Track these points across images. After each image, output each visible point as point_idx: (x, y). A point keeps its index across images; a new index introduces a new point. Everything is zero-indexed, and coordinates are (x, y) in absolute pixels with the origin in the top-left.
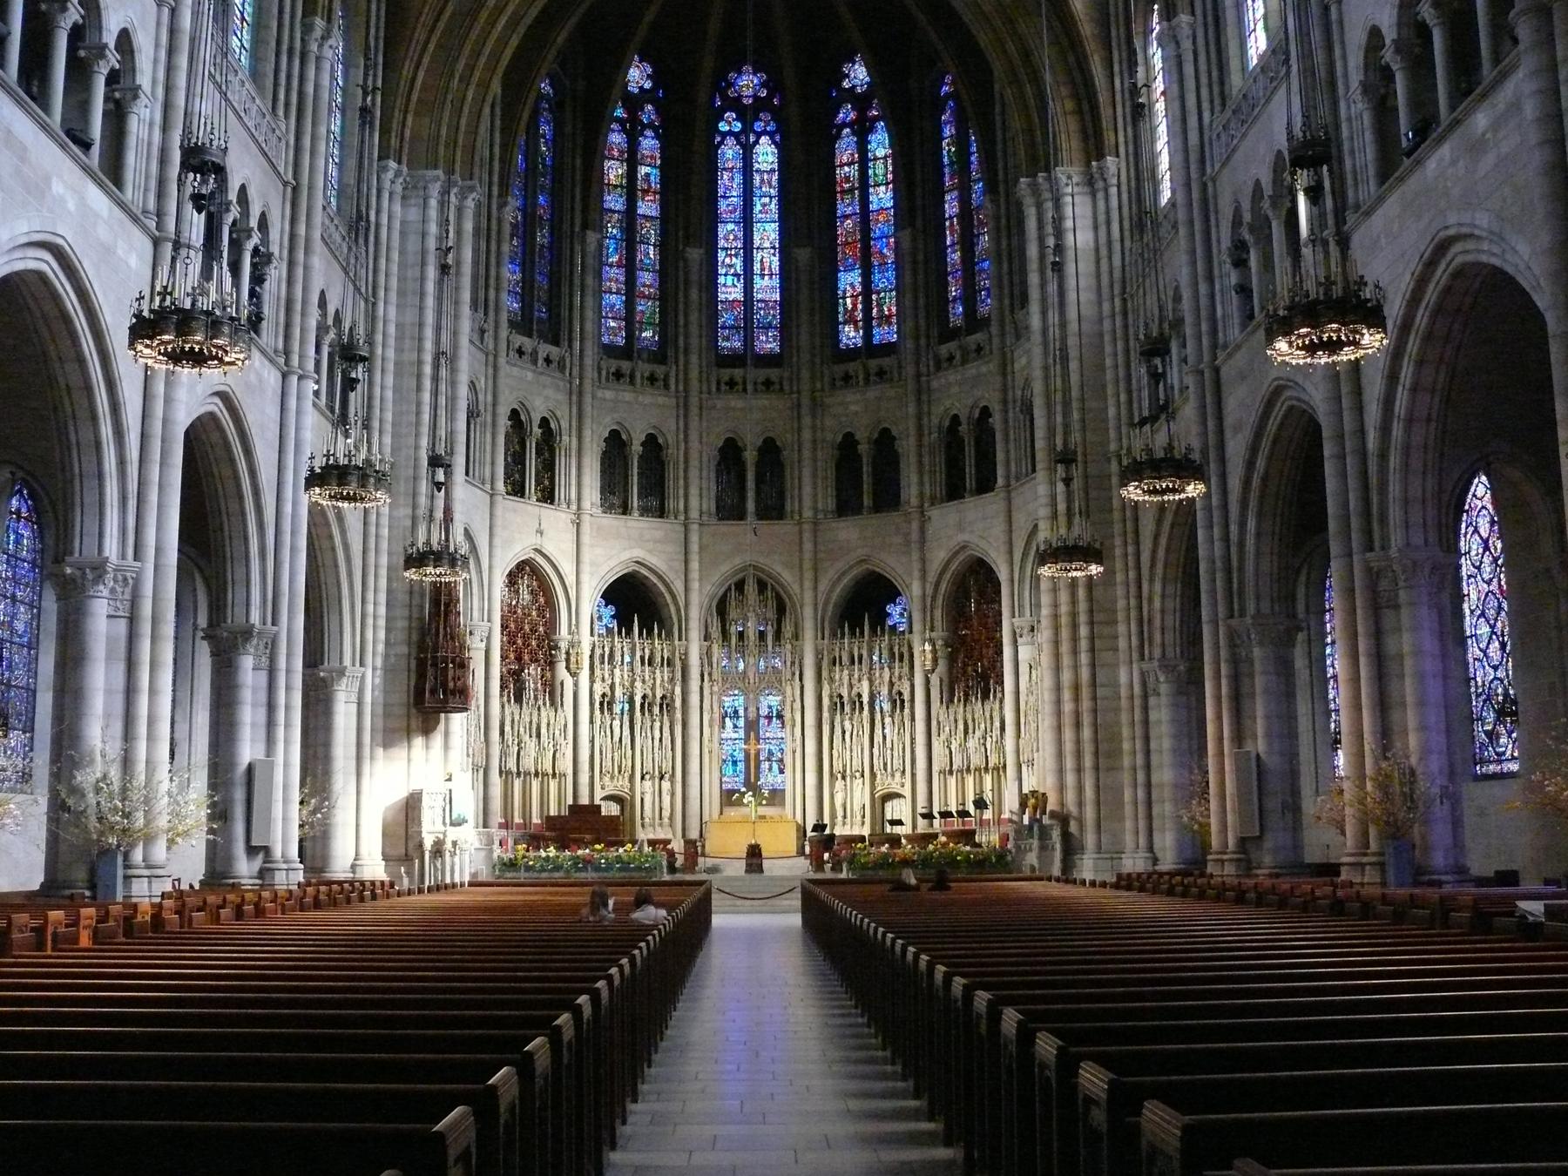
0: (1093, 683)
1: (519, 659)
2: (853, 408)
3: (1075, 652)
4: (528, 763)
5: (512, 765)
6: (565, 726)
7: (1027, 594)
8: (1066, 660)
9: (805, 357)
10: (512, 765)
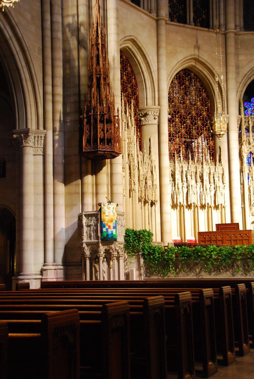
1: (189, 133)
4: (194, 199)
5: (181, 199)
6: (223, 174)
10: (181, 199)
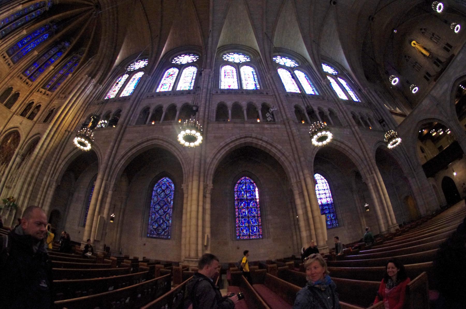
0: (37, 177)
2: (18, 84)
3: (37, 167)
7: (26, 146)
8: (34, 167)
9: (19, 67)
